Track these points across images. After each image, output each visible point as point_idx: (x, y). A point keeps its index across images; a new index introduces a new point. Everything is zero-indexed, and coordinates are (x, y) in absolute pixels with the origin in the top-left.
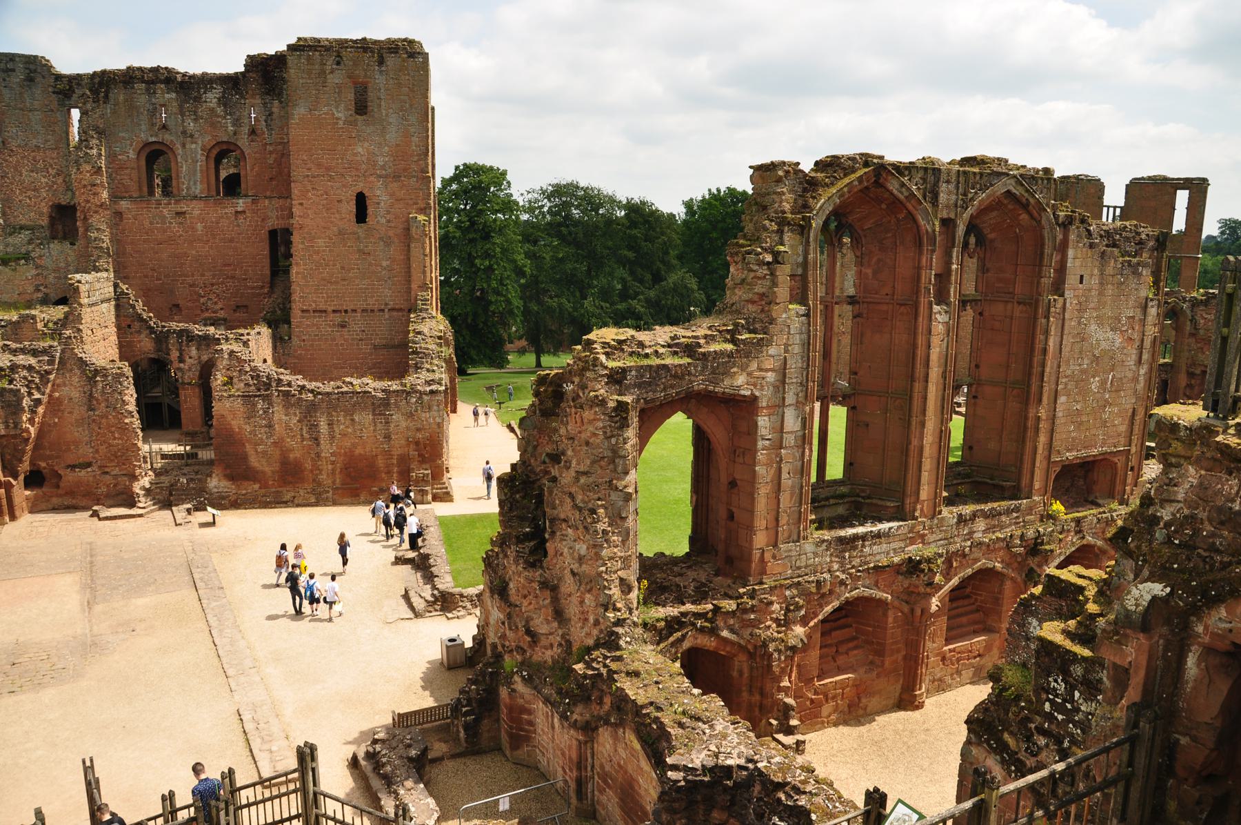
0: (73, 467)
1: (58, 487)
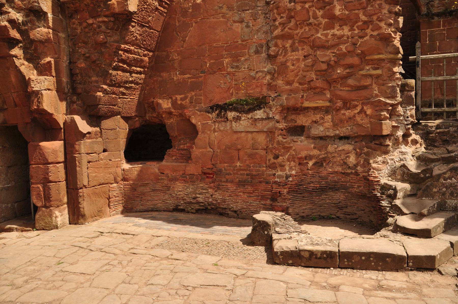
0: (221, 109)
1: (187, 158)
